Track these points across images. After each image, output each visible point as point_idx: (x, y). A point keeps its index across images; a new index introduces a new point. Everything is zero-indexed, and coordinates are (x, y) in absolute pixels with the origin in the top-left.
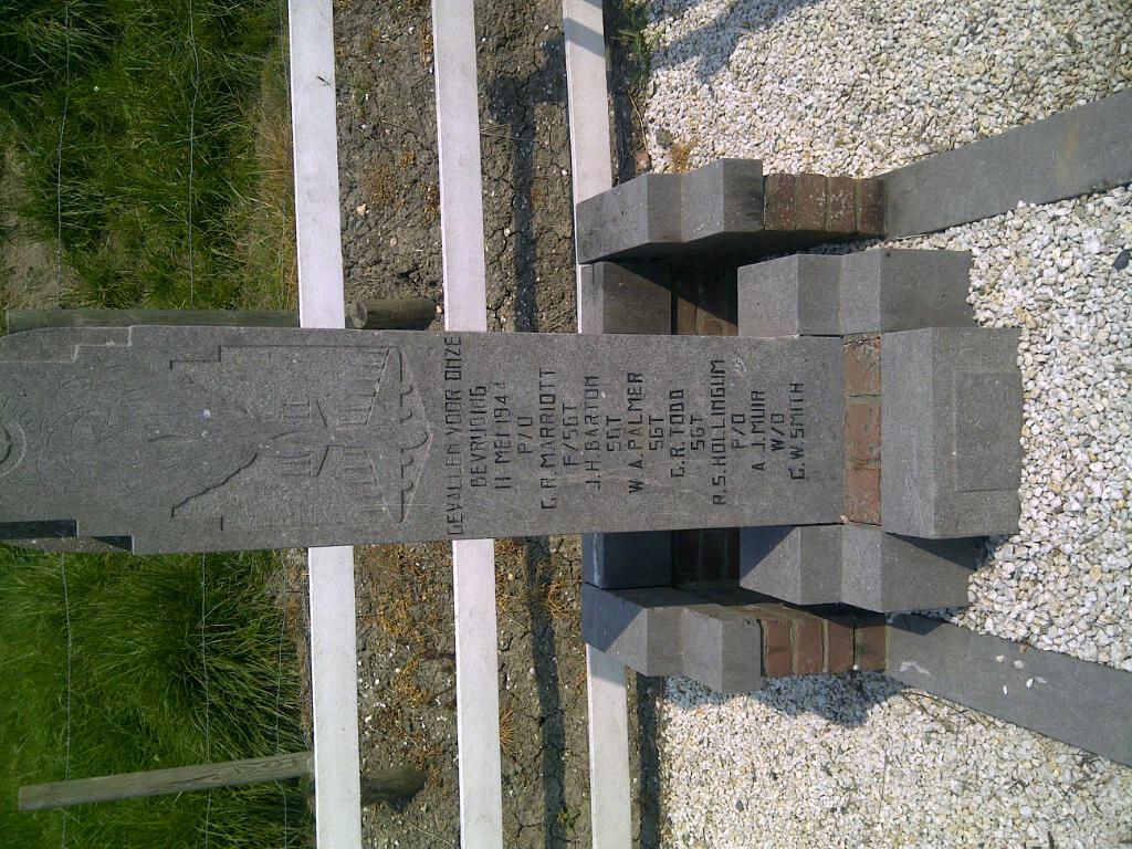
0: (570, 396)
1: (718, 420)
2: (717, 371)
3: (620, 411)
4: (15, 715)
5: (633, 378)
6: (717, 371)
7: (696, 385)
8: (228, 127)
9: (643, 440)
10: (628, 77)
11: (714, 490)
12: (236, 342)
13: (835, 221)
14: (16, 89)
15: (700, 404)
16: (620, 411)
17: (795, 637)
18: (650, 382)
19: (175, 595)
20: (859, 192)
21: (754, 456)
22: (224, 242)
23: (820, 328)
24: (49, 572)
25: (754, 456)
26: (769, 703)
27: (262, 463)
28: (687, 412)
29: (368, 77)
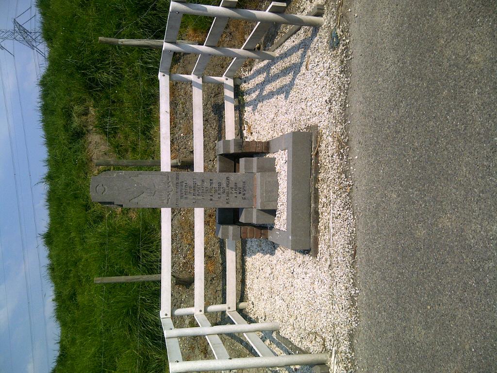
1: (228, 188)
4: (88, 275)
8: (152, 107)
9: (213, 192)
10: (240, 108)
12: (140, 174)
13: (258, 150)
15: (224, 185)
17: (248, 231)
18: (214, 181)
19: (135, 236)
22: (150, 139)
24: (100, 231)
26: (262, 253)
27: (144, 194)
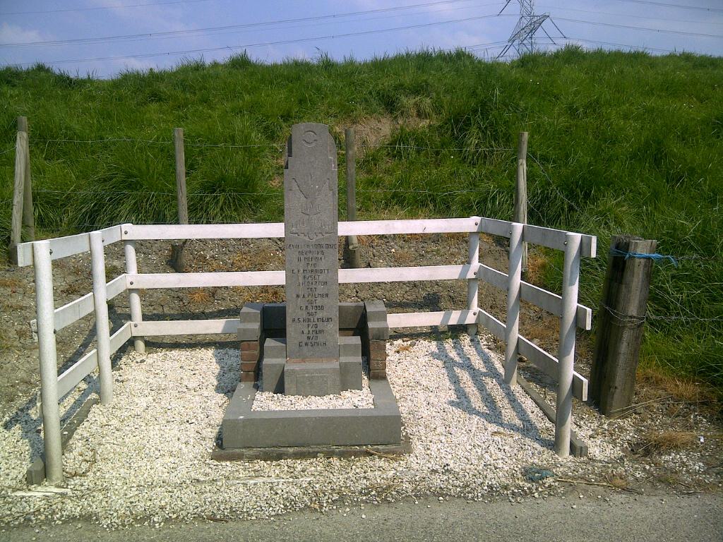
0: (322, 278)
1: (316, 320)
2: (329, 320)
3: (318, 292)
4: (187, 118)
5: (327, 295)
6: (329, 320)
7: (325, 314)
8: (431, 206)
9: (310, 298)
10: (434, 334)
11: (296, 319)
12: (334, 194)
13: (373, 363)
14: (452, 126)
15: (320, 314)
16: (318, 292)
17: (251, 352)
18: (326, 300)
19: (246, 185)
20: (382, 371)
21: (306, 331)
22: (387, 205)
23: (342, 351)
24: (253, 135)
25: (306, 331)
26: (219, 374)
27: (305, 199)
28: (318, 311)
29: (442, 253)
